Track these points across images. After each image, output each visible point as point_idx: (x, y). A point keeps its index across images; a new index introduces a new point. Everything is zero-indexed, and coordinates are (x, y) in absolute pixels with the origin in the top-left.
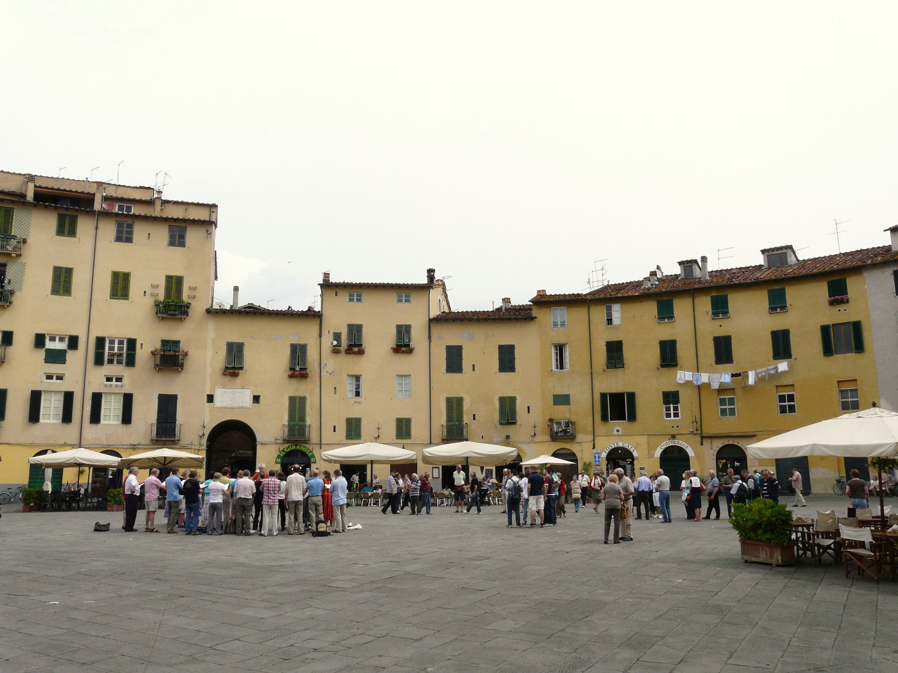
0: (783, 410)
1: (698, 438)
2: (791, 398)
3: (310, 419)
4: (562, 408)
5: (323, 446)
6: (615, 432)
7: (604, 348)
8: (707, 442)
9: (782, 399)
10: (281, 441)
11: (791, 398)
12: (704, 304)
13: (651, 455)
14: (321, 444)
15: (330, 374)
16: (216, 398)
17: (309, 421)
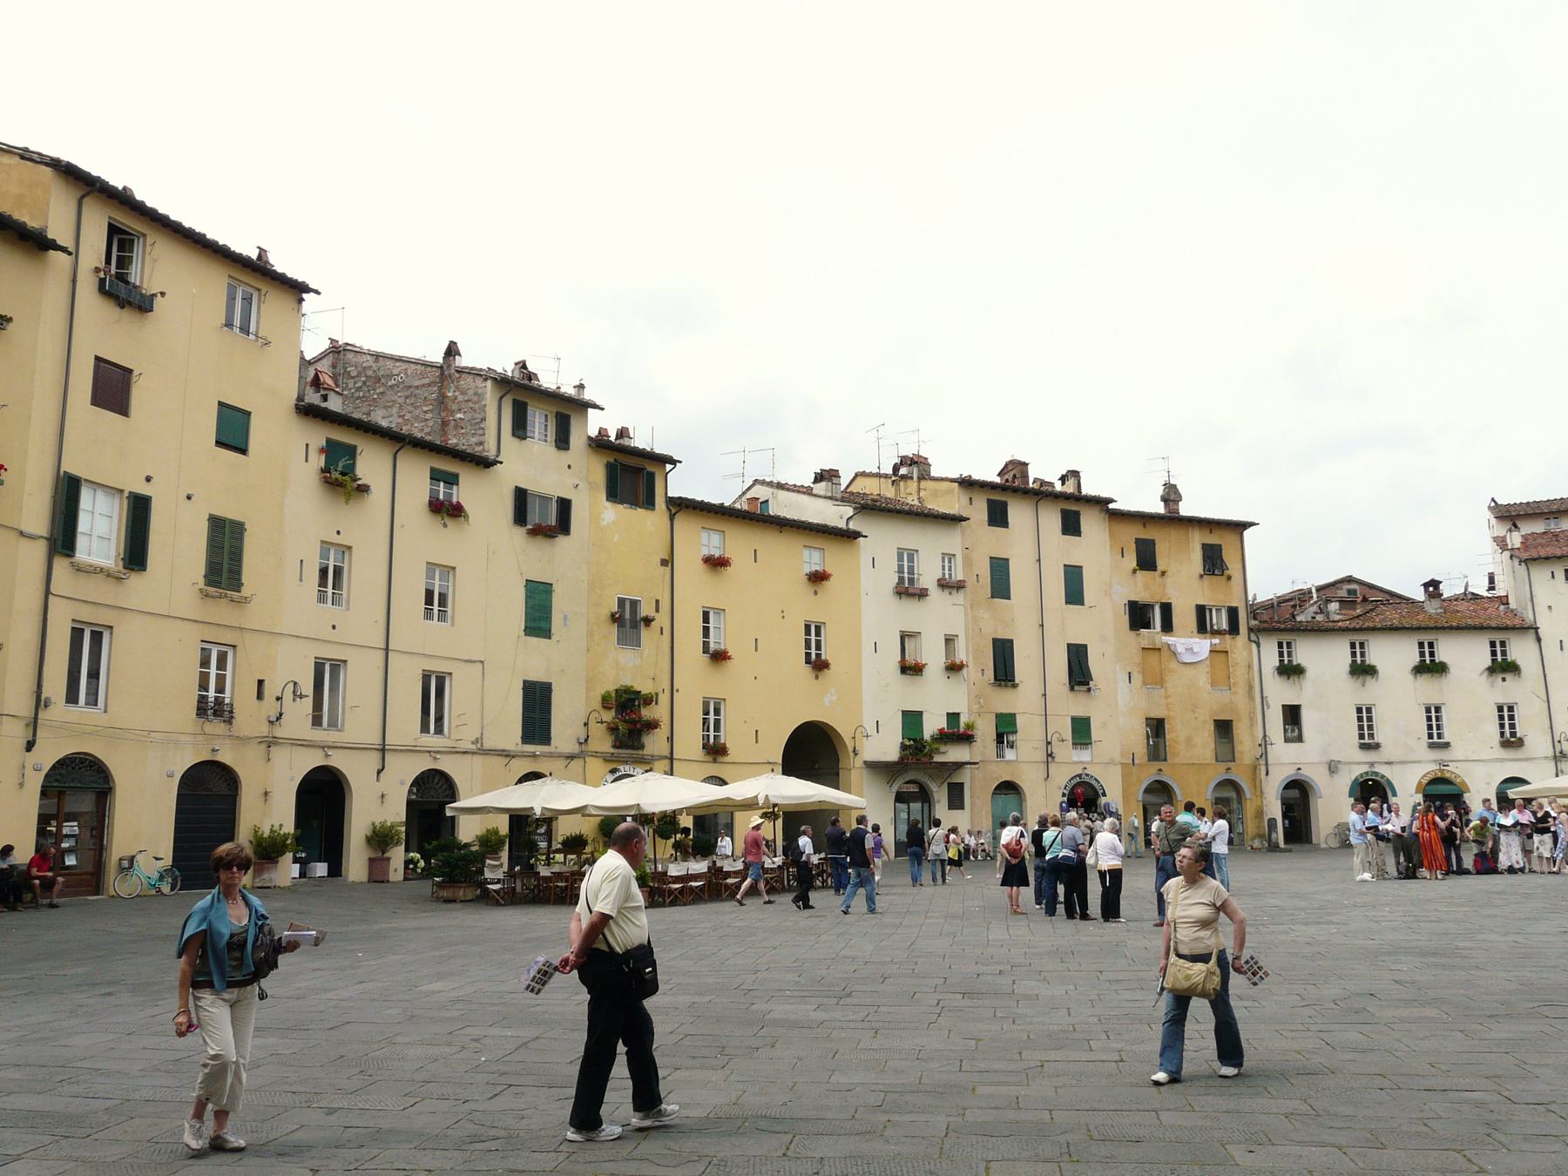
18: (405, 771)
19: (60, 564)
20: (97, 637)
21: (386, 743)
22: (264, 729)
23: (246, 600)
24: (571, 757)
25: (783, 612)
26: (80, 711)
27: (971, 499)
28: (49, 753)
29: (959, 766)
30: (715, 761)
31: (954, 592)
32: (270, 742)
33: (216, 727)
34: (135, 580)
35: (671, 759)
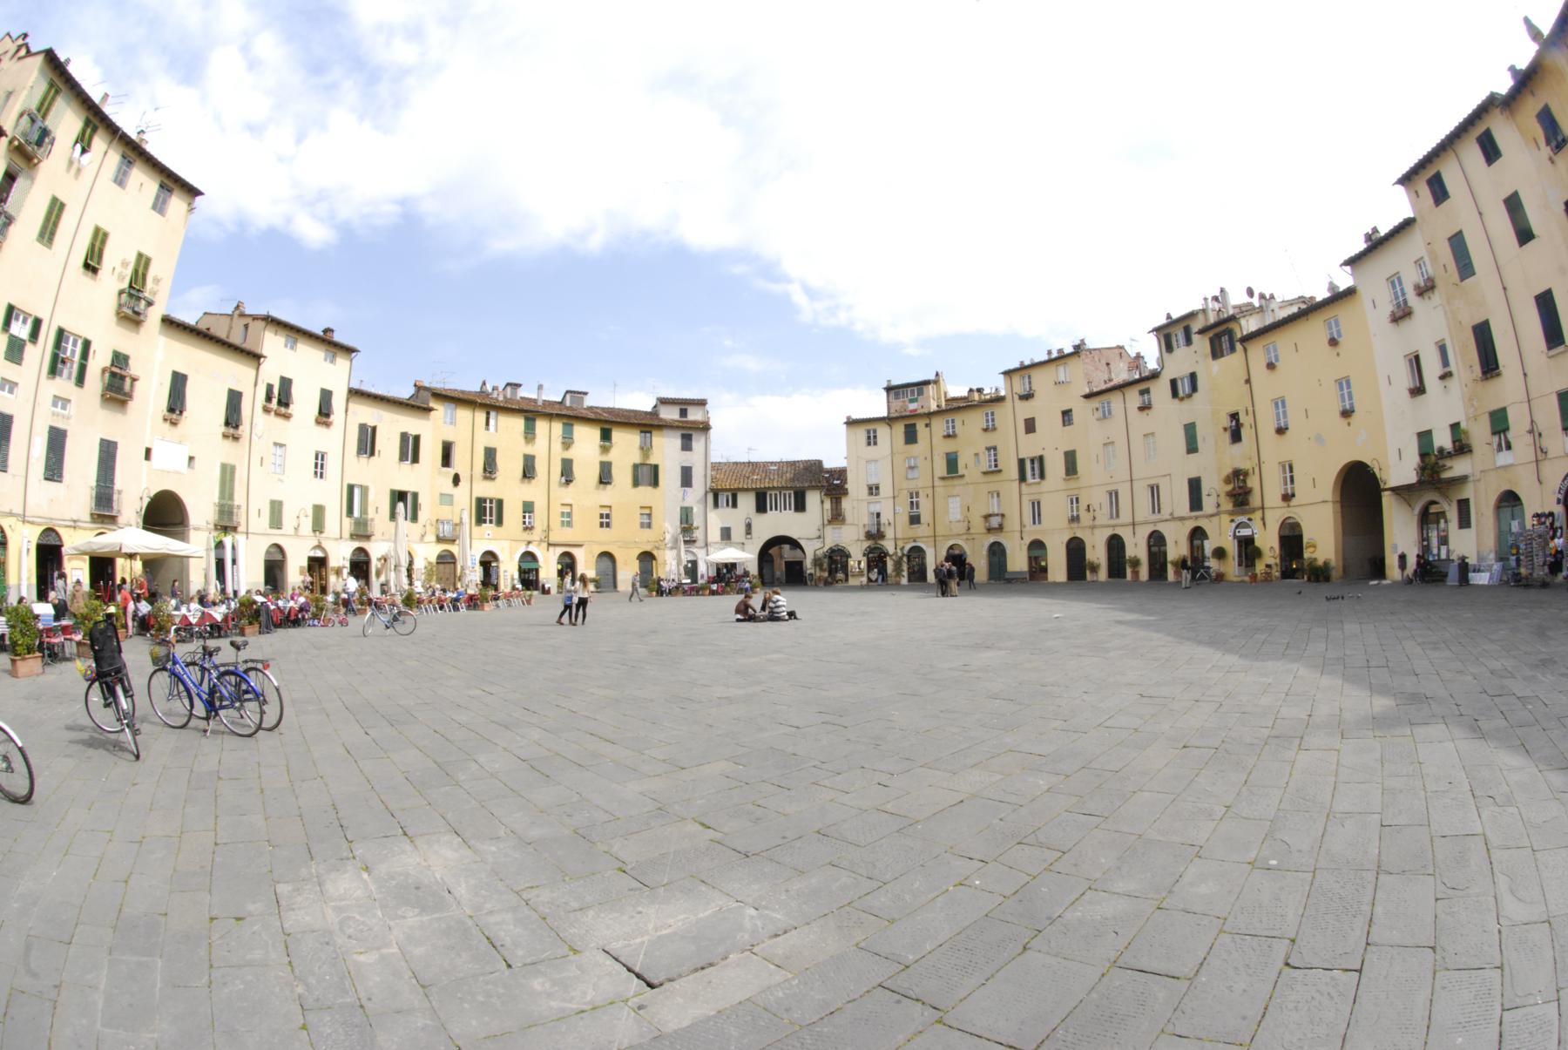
0: (602, 525)
1: (545, 545)
2: (608, 516)
3: (239, 499)
4: (446, 508)
5: (250, 535)
6: (487, 537)
7: (483, 453)
8: (551, 549)
9: (602, 516)
10: (212, 526)
11: (608, 516)
12: (558, 427)
13: (512, 559)
14: (247, 533)
15: (260, 438)
16: (154, 454)
17: (237, 502)
18: (1144, 532)
19: (1023, 485)
20: (1039, 503)
21: (1136, 520)
22: (1091, 523)
23: (1078, 478)
24: (1212, 516)
25: (1319, 381)
26: (1037, 527)
27: (1416, 192)
28: (1027, 540)
29: (1462, 480)
30: (1289, 506)
31: (1430, 294)
32: (1093, 527)
33: (1075, 525)
34: (1044, 482)
35: (1263, 508)
